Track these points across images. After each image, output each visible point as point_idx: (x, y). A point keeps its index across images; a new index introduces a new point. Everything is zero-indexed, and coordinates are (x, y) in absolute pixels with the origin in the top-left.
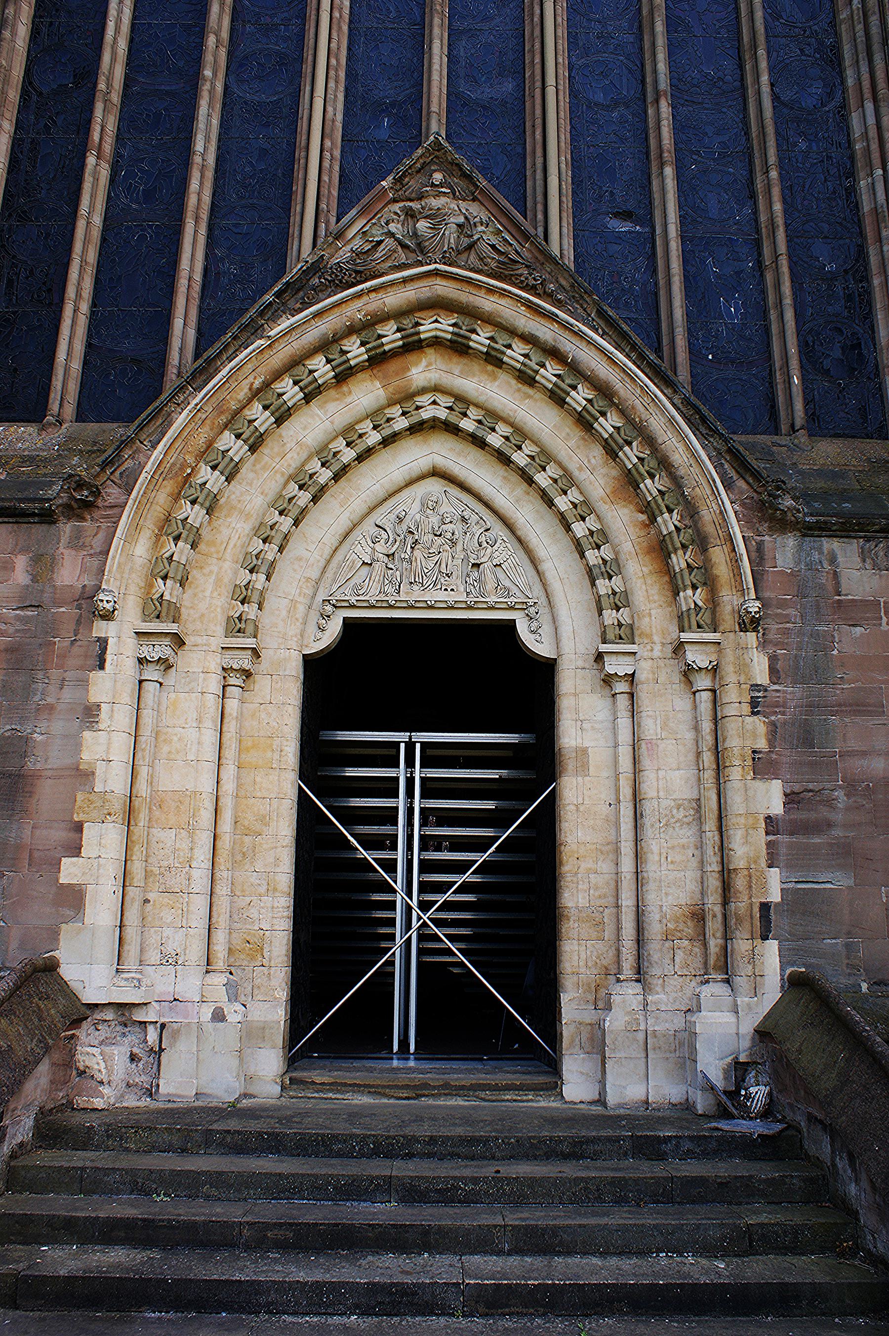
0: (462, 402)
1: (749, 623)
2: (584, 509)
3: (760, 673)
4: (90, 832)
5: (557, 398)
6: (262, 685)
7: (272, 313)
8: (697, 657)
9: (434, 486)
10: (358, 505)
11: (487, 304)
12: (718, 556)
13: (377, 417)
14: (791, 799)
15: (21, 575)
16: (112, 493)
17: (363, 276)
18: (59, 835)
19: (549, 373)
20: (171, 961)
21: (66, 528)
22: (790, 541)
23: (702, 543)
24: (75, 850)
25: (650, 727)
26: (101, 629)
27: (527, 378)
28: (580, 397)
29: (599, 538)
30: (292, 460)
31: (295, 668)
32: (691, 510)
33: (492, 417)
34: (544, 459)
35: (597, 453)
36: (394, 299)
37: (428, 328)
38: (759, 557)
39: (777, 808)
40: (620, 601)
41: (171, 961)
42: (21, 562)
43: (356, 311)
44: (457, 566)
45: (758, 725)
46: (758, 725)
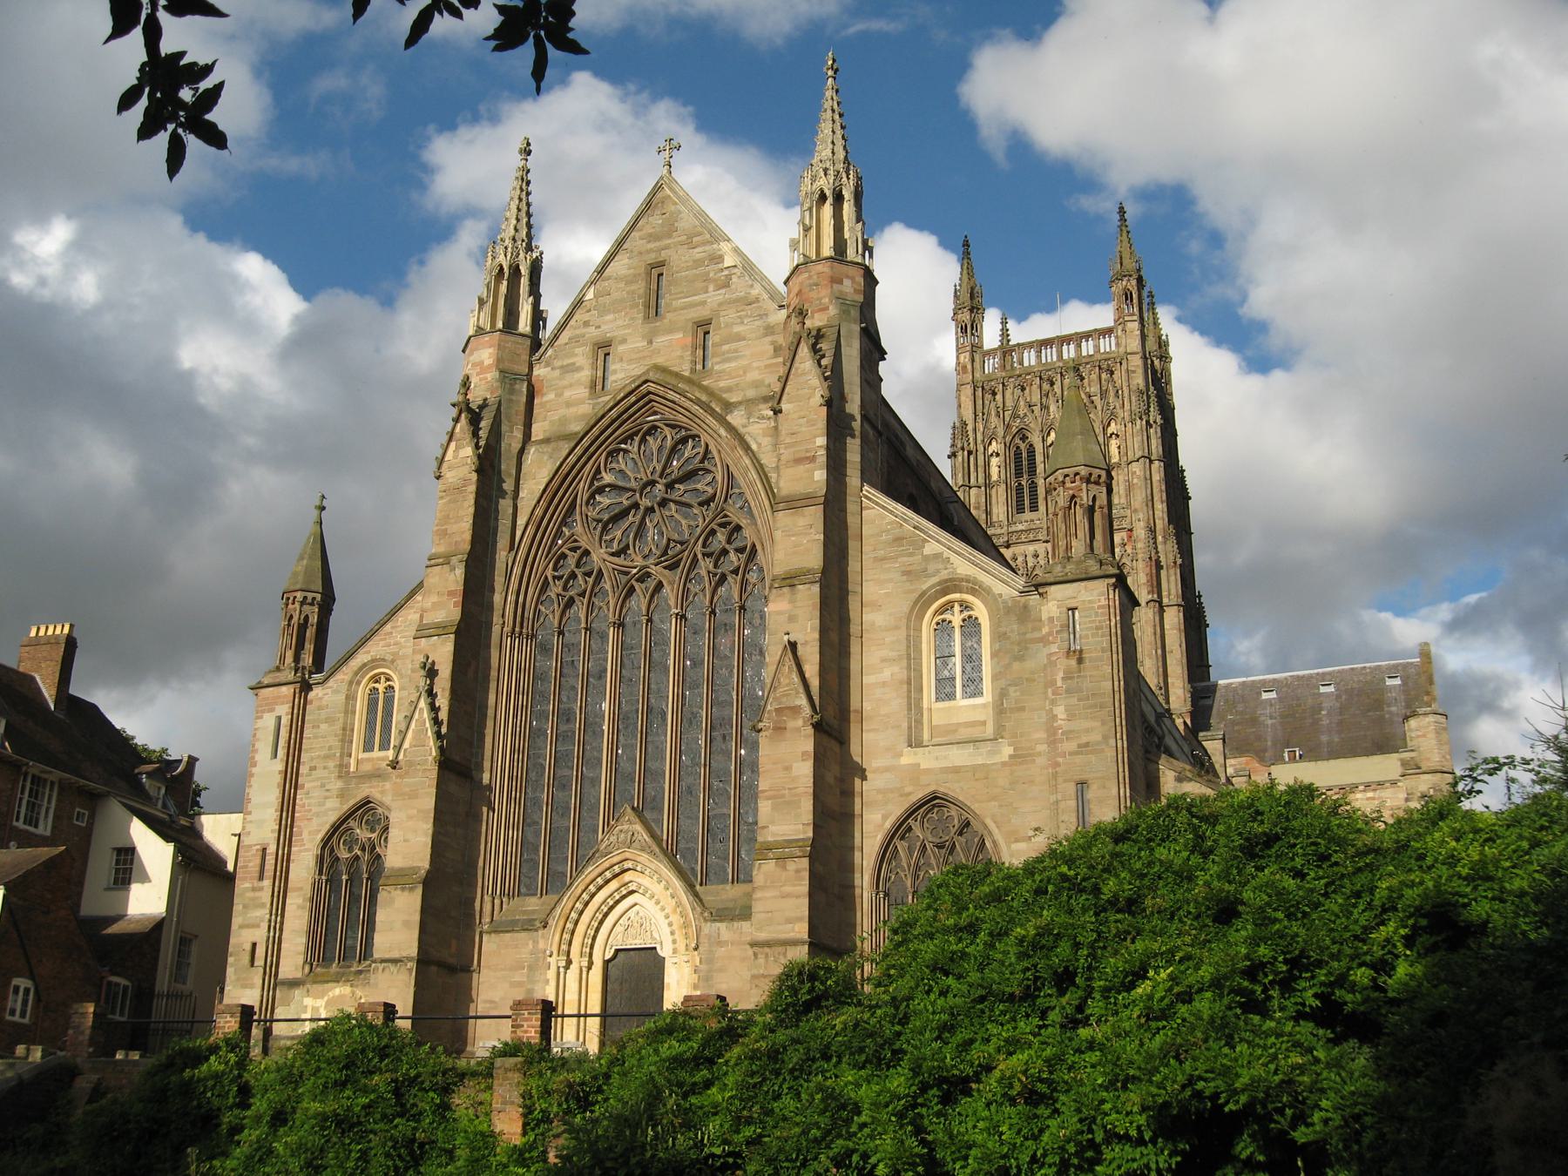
42: (531, 942)
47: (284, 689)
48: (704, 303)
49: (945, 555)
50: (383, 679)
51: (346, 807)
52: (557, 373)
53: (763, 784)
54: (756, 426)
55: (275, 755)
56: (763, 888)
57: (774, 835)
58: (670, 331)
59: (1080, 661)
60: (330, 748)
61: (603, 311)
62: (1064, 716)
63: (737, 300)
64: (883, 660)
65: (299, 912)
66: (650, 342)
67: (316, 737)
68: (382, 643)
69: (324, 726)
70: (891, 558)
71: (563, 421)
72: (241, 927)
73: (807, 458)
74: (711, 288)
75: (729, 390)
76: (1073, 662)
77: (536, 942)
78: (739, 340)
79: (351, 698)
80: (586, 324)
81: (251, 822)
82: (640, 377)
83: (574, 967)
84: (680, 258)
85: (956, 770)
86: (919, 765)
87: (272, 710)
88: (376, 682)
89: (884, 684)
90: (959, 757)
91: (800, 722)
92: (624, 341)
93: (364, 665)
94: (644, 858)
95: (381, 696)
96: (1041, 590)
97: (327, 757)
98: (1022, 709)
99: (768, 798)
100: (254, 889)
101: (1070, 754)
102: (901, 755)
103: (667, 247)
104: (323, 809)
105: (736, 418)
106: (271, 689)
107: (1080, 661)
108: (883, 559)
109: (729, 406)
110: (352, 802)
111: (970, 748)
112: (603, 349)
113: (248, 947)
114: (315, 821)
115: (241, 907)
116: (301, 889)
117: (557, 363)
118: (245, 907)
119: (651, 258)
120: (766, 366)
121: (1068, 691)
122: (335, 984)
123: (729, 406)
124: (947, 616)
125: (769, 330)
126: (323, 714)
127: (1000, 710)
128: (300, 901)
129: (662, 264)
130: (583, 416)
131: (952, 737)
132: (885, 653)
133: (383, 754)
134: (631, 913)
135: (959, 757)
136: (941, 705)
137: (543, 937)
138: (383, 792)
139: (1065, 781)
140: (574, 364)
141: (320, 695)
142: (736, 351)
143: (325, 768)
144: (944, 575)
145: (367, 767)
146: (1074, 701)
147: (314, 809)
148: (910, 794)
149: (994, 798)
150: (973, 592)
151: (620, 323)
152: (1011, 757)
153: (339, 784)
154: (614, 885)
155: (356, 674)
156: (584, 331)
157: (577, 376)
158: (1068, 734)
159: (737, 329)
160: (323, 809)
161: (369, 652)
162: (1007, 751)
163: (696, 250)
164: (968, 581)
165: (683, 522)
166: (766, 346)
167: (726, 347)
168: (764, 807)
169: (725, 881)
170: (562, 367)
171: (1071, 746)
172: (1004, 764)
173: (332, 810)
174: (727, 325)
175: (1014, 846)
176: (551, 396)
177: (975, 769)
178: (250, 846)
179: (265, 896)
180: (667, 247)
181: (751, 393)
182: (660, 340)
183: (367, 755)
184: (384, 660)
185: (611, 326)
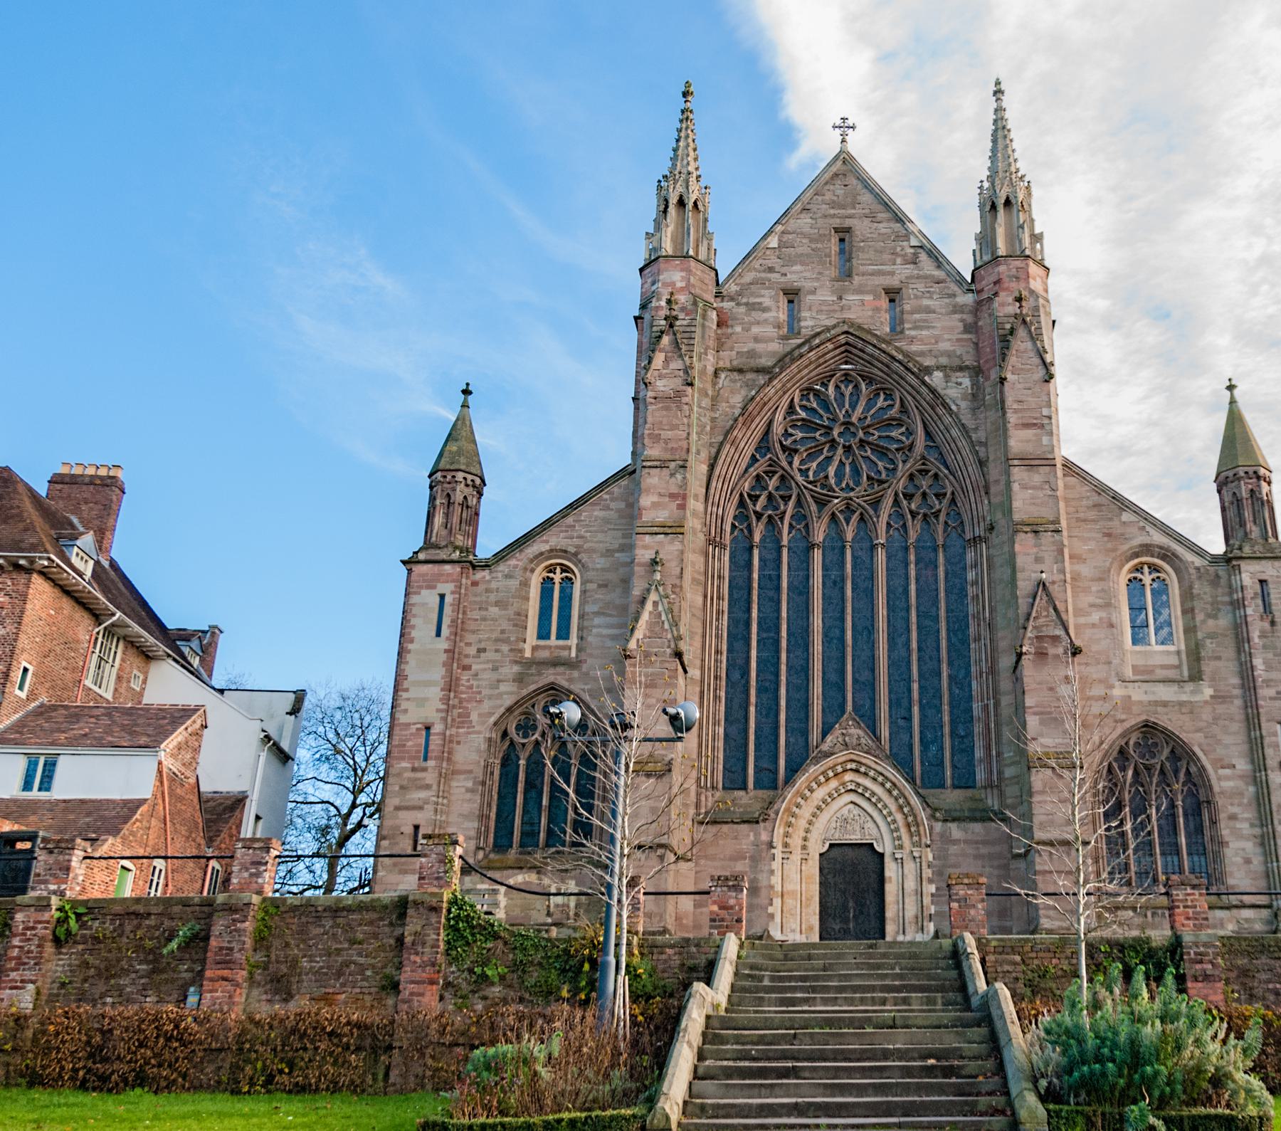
0: (858, 785)
1: (928, 846)
2: (890, 814)
3: (930, 857)
4: (775, 900)
5: (883, 785)
6: (810, 862)
7: (809, 765)
8: (916, 854)
9: (851, 806)
10: (832, 812)
11: (864, 761)
12: (921, 828)
13: (837, 790)
14: (937, 889)
15: (752, 838)
16: (773, 815)
17: (832, 754)
18: (767, 901)
19: (880, 779)
20: (793, 931)
21: (762, 825)
22: (940, 824)
23: (918, 825)
24: (771, 905)
25: (906, 871)
26: (773, 851)
27: (875, 779)
28: (888, 785)
29: (894, 821)
30: (815, 803)
31: (817, 857)
32: (915, 816)
33: (866, 789)
34: (880, 800)
35: (892, 800)
36: (840, 760)
37: (849, 767)
38: (931, 829)
39: (934, 891)
40: (899, 838)
41: (793, 931)
43: (831, 764)
44: (858, 828)
45: (930, 871)
46: (930, 871)
47: (447, 567)
48: (892, 273)
49: (1142, 524)
50: (558, 570)
51: (525, 692)
52: (742, 309)
53: (1029, 701)
54: (954, 390)
55: (438, 634)
56: (1043, 792)
57: (1042, 746)
58: (859, 291)
59: (1273, 623)
60: (503, 632)
61: (790, 261)
62: (1262, 667)
63: (926, 277)
64: (1092, 606)
65: (468, 796)
66: (840, 298)
67: (484, 619)
68: (562, 535)
69: (494, 611)
70: (1093, 521)
71: (752, 354)
72: (397, 808)
73: (1035, 425)
74: (899, 261)
75: (922, 354)
76: (1267, 625)
77: (757, 835)
78: (930, 312)
79: (525, 584)
80: (771, 270)
81: (408, 699)
82: (834, 327)
83: (796, 857)
84: (861, 227)
85: (1165, 704)
86: (1130, 697)
87: (434, 587)
88: (550, 571)
89: (1094, 625)
90: (1166, 693)
91: (1060, 650)
92: (813, 292)
93: (542, 554)
94: (869, 760)
95: (557, 587)
96: (1234, 563)
97: (497, 640)
98: (1219, 658)
99: (1035, 714)
100: (414, 769)
101: (1271, 698)
102: (1112, 687)
103: (850, 217)
104: (497, 691)
105: (936, 379)
106: (430, 566)
107: (1273, 623)
108: (1085, 521)
109: (928, 370)
110: (532, 687)
111: (1175, 687)
112: (792, 295)
113: (409, 830)
114: (486, 705)
115: (397, 788)
116: (470, 772)
117: (744, 300)
118: (402, 787)
119: (837, 222)
120: (958, 340)
121: (1264, 647)
122: (516, 871)
123: (928, 370)
124: (1139, 575)
125: (957, 309)
126: (493, 597)
127: (1195, 654)
128: (470, 784)
129: (848, 230)
130: (774, 353)
131: (1146, 676)
132: (1091, 599)
133: (561, 642)
134: (845, 811)
135: (1166, 693)
136: (1138, 648)
137: (765, 828)
138: (568, 680)
139: (1268, 721)
140: (760, 303)
141: (488, 578)
142: (925, 321)
143: (497, 651)
144: (1146, 540)
145: (544, 654)
146: (1270, 656)
147: (485, 692)
148: (1123, 721)
149: (1199, 730)
150: (1164, 557)
151: (808, 274)
152: (1212, 697)
153: (516, 668)
154: (834, 784)
155: (531, 561)
156: (769, 275)
157: (766, 315)
158: (1268, 683)
159: (926, 302)
160: (497, 691)
161: (547, 542)
162: (1208, 692)
163: (881, 225)
164: (1161, 548)
165: (880, 464)
166: (955, 322)
167: (917, 316)
168: (1032, 722)
169: (942, 786)
170: (747, 304)
171: (1271, 692)
172: (1206, 702)
173: (509, 694)
174: (916, 297)
175: (1221, 772)
176: (738, 329)
177: (1181, 704)
178: (409, 724)
179: (430, 777)
180: (850, 217)
181: (944, 361)
182: (851, 297)
183: (542, 643)
184: (565, 551)
185: (796, 275)
